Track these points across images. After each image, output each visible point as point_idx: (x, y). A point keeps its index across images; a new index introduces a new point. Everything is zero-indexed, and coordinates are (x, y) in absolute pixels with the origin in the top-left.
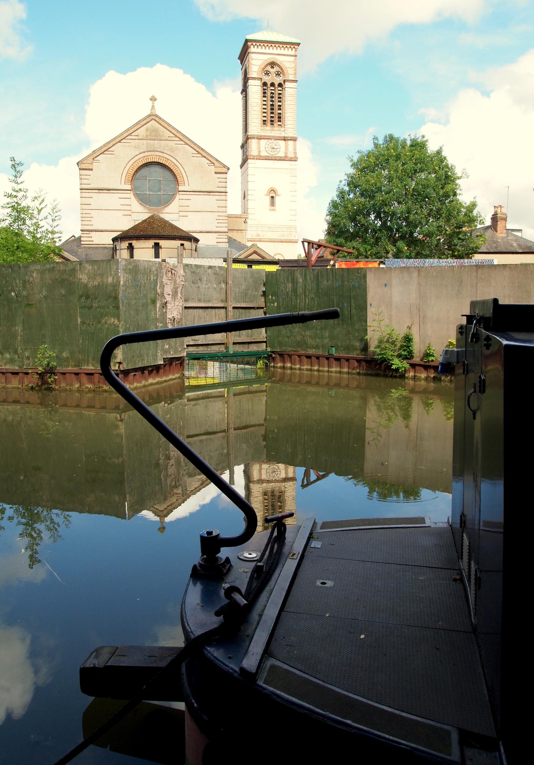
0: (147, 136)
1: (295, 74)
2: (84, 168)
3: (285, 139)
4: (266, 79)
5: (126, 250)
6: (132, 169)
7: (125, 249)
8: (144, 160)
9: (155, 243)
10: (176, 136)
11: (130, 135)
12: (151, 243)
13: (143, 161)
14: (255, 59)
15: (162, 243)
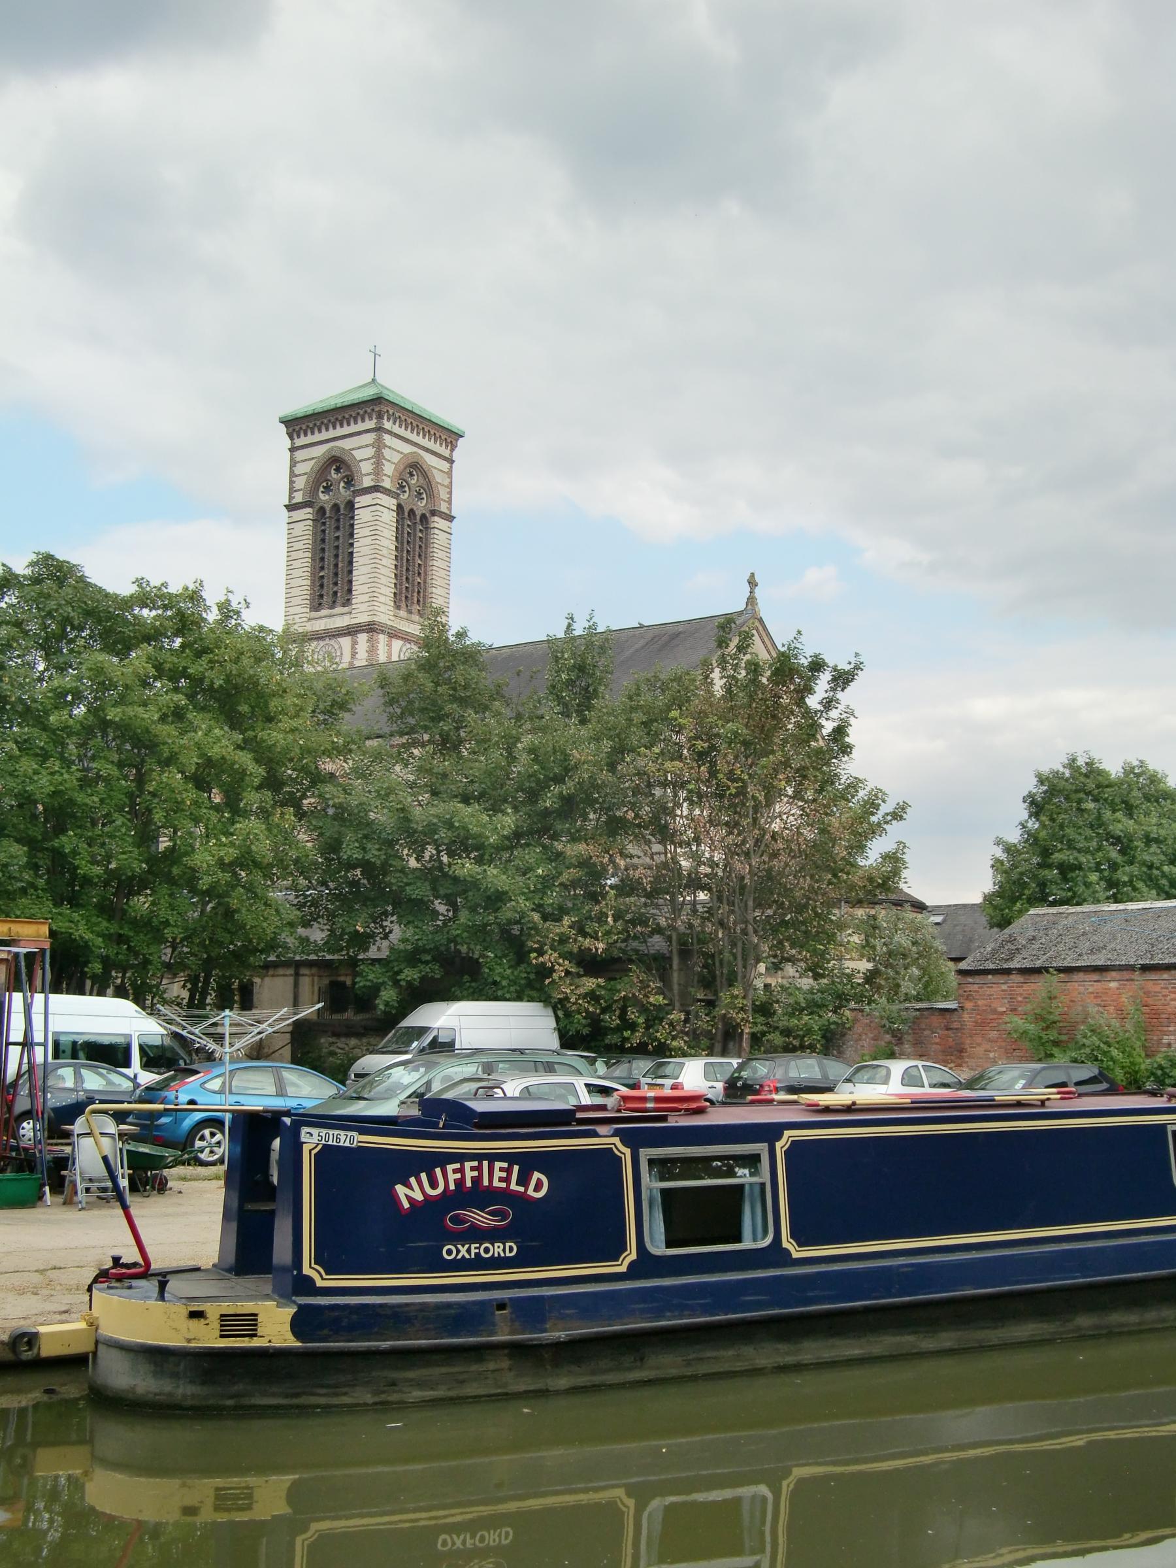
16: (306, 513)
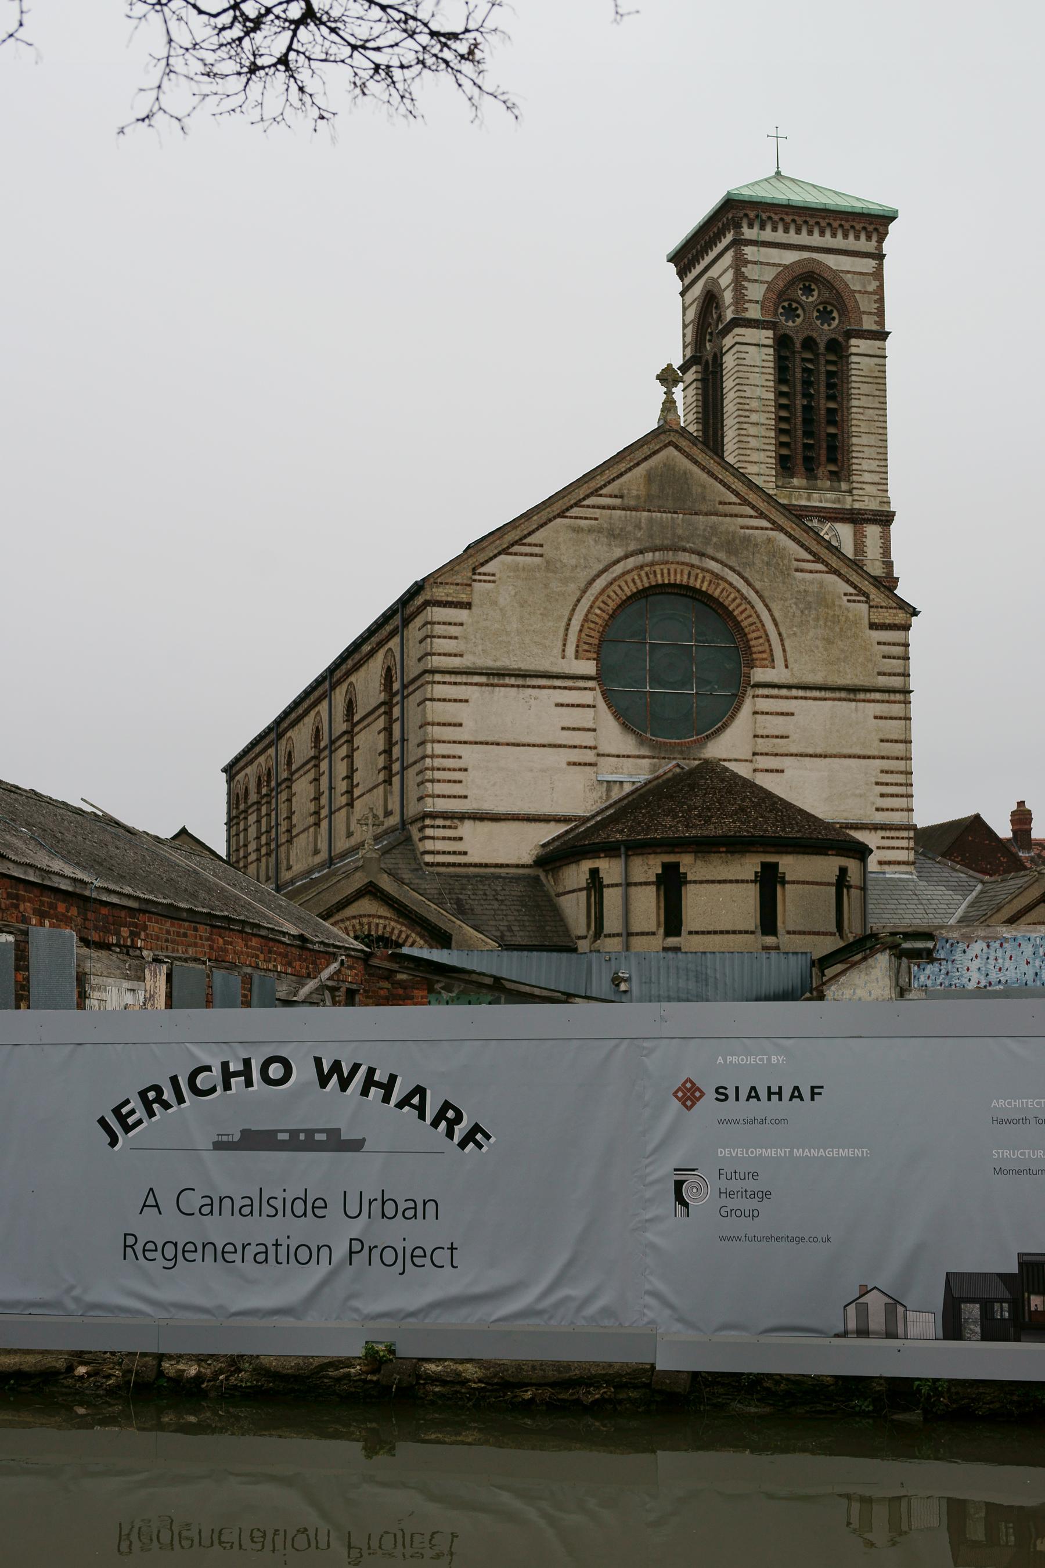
0: (649, 497)
1: (880, 313)
2: (444, 599)
3: (856, 518)
4: (789, 325)
5: (654, 888)
6: (602, 605)
7: (646, 884)
8: (639, 575)
9: (764, 865)
10: (745, 502)
11: (595, 492)
12: (749, 866)
13: (638, 581)
14: (755, 263)
15: (790, 865)
16: (765, 336)
